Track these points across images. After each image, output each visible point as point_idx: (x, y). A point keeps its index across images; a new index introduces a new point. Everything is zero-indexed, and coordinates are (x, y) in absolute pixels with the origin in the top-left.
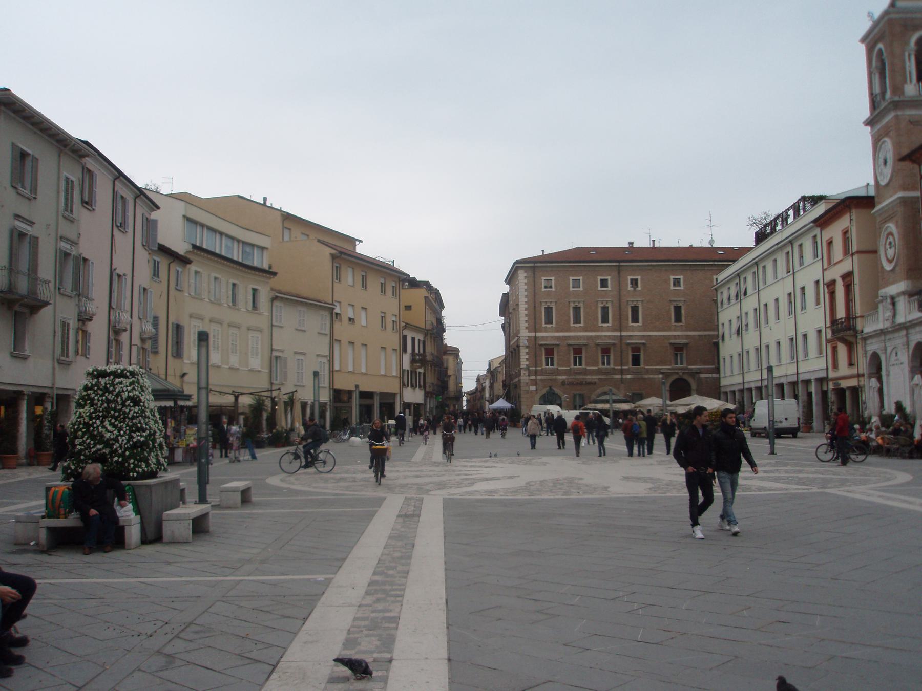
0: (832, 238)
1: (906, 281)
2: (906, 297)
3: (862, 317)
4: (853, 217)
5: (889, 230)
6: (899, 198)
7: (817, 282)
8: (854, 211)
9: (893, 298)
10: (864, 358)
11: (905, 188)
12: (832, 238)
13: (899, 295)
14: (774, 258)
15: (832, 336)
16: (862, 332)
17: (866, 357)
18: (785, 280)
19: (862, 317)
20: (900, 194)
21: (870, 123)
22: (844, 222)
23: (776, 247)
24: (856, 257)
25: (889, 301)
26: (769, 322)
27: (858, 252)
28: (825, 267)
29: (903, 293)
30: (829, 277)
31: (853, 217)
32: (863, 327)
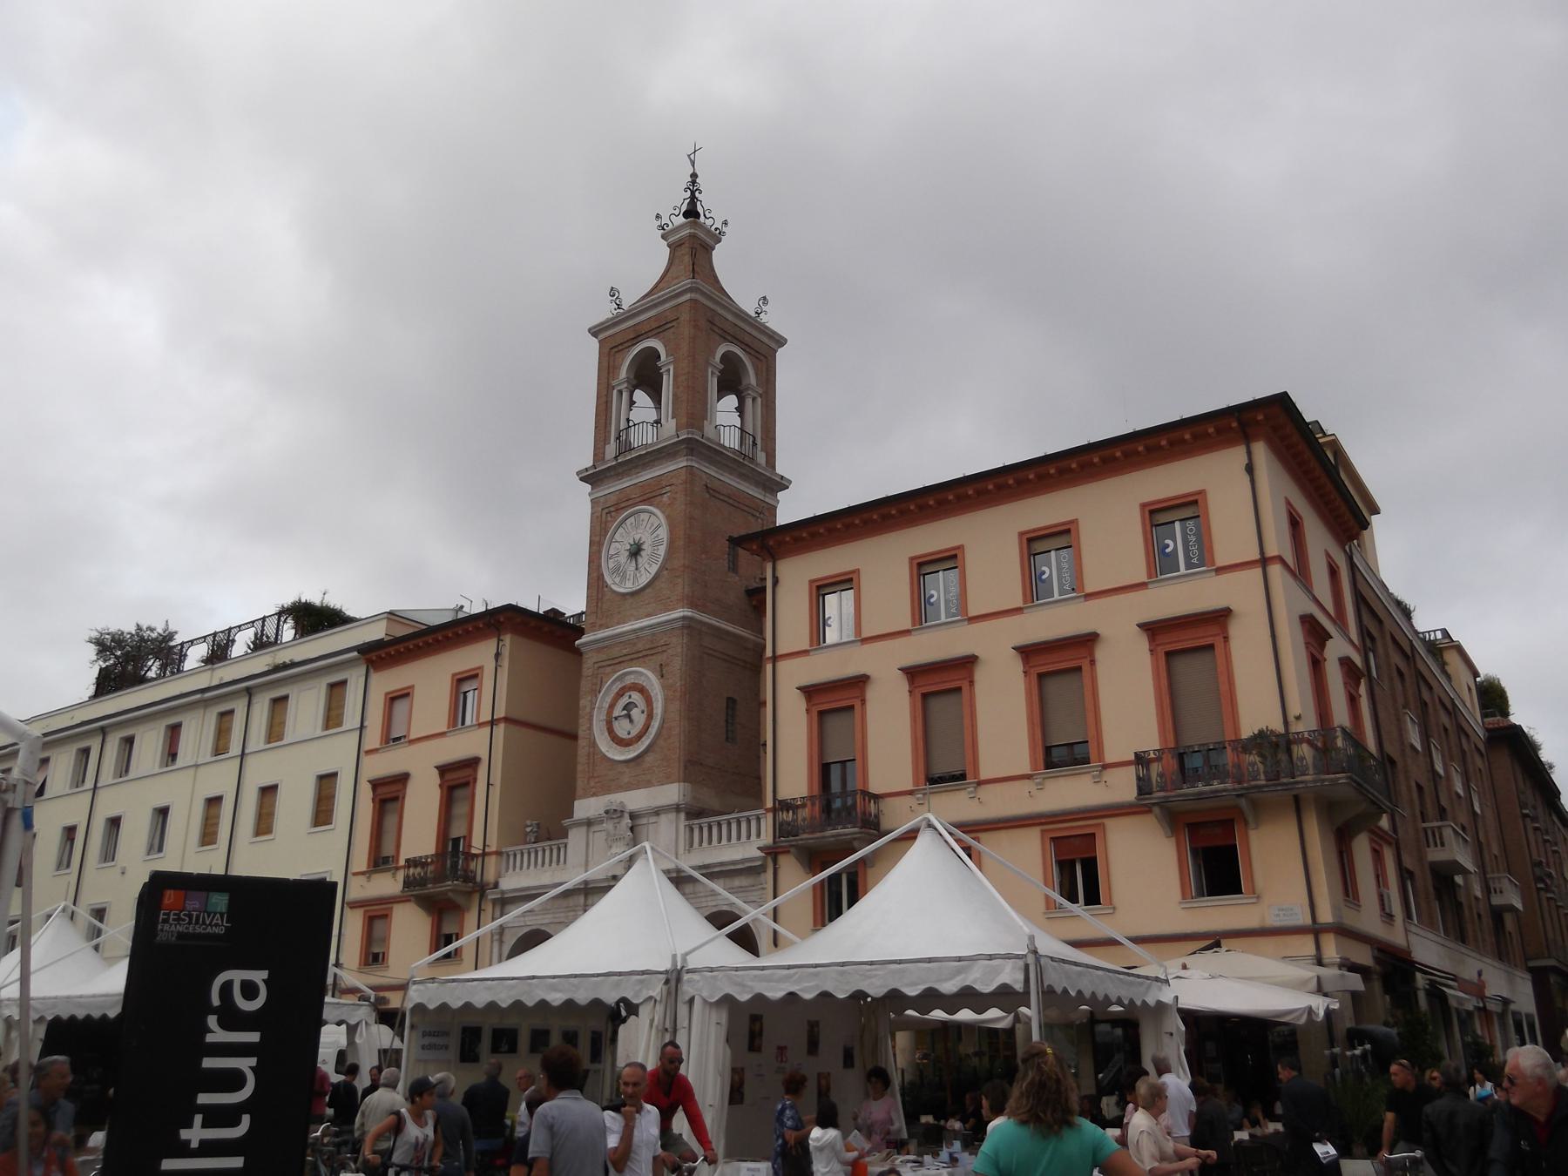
0: (412, 687)
1: (682, 784)
2: (682, 816)
3: (498, 853)
4: (506, 652)
5: (629, 680)
6: (684, 618)
7: (326, 782)
8: (507, 639)
9: (633, 816)
10: (496, 945)
11: (692, 605)
12: (412, 687)
13: (657, 812)
14: (173, 720)
15: (403, 891)
16: (496, 885)
17: (501, 942)
18: (202, 769)
19: (498, 853)
20: (688, 612)
21: (592, 478)
22: (479, 655)
23: (198, 696)
24: (500, 730)
25: (627, 821)
26: (116, 859)
27: (506, 720)
28: (367, 746)
29: (677, 808)
30: (384, 764)
31: (506, 652)
32: (499, 875)
